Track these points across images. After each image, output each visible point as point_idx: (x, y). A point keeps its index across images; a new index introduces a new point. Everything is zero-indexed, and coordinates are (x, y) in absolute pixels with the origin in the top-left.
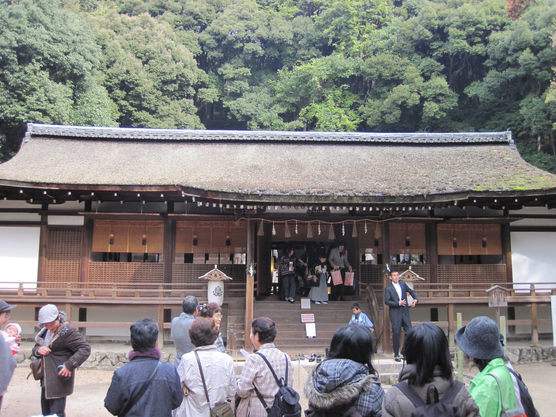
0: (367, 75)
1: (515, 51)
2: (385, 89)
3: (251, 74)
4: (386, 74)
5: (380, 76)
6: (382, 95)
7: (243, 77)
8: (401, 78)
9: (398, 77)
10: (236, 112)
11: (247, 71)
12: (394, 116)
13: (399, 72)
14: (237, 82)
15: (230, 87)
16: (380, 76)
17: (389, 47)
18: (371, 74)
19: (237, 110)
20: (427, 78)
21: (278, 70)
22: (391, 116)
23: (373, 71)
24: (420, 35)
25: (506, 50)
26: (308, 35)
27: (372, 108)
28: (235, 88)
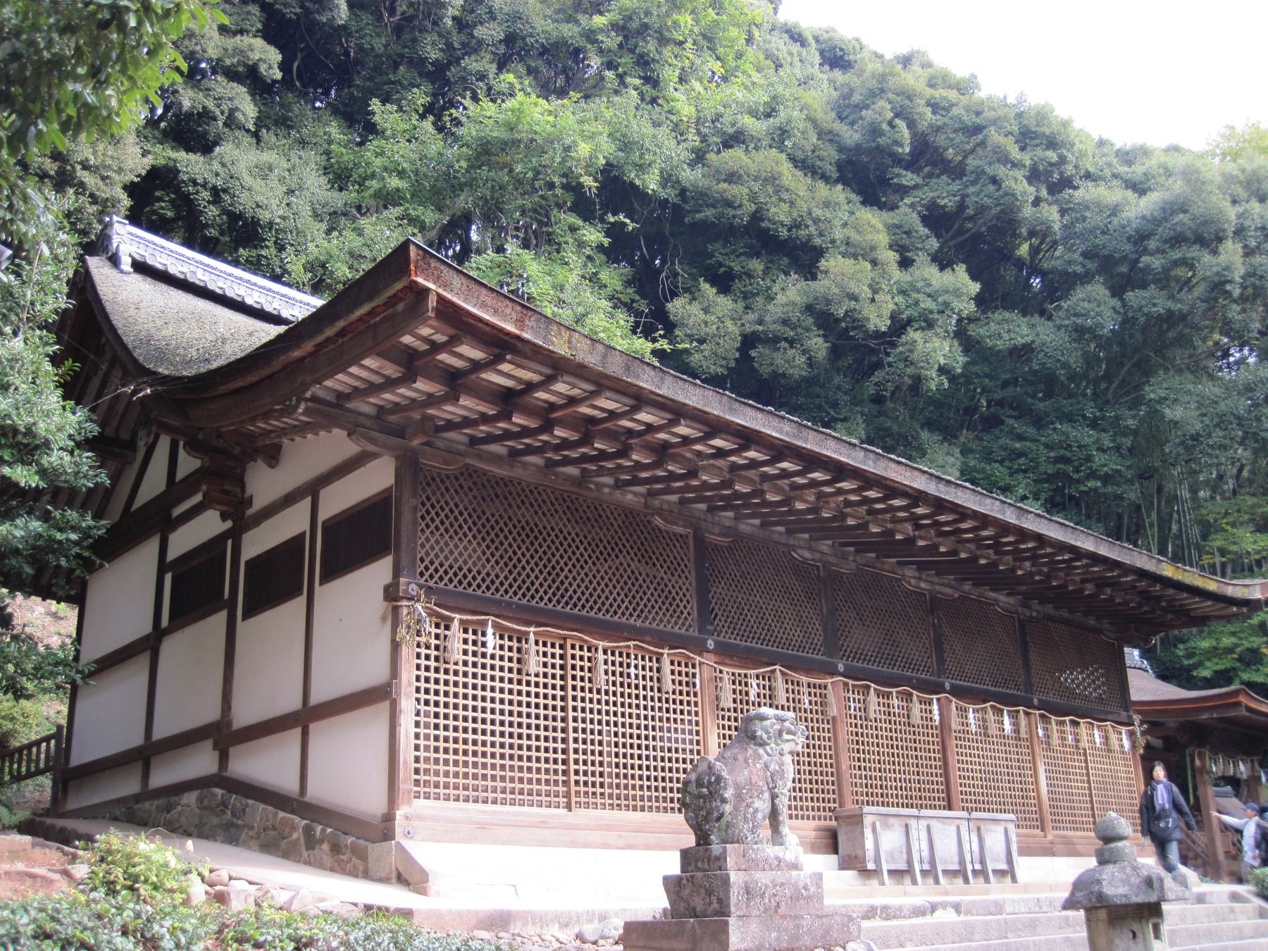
0: (714, 206)
1: (1177, 240)
2: (756, 265)
3: (278, 75)
4: (780, 213)
5: (757, 216)
6: (737, 285)
7: (250, 76)
8: (817, 241)
9: (810, 236)
10: (206, 195)
11: (268, 58)
12: (804, 352)
13: (816, 221)
14: (221, 86)
15: (190, 93)
16: (757, 216)
17: (780, 136)
18: (728, 204)
19: (216, 193)
20: (905, 263)
21: (375, 105)
22: (791, 352)
23: (737, 192)
24: (875, 131)
25: (1140, 238)
26: (516, 17)
27: (707, 315)
28: (210, 104)
